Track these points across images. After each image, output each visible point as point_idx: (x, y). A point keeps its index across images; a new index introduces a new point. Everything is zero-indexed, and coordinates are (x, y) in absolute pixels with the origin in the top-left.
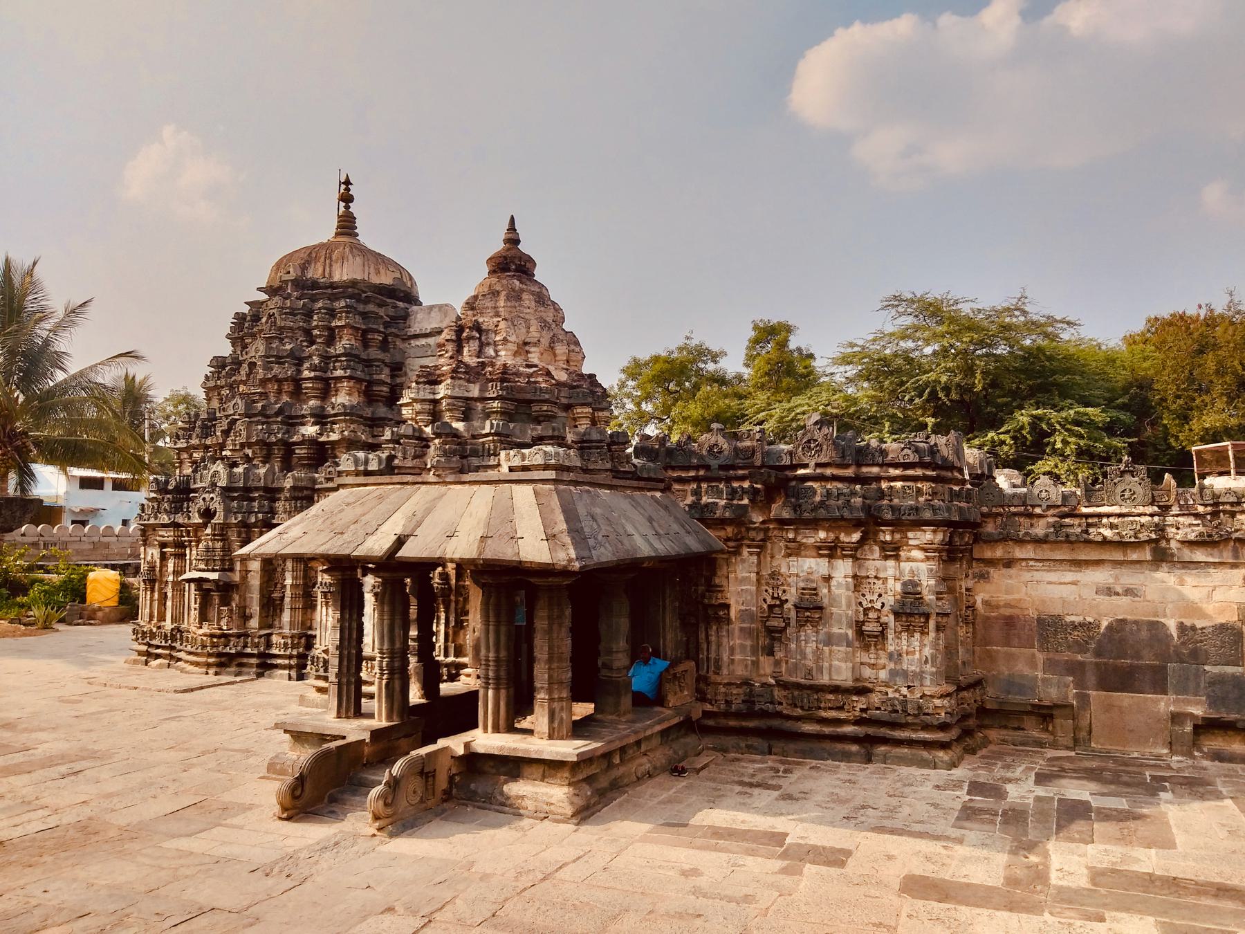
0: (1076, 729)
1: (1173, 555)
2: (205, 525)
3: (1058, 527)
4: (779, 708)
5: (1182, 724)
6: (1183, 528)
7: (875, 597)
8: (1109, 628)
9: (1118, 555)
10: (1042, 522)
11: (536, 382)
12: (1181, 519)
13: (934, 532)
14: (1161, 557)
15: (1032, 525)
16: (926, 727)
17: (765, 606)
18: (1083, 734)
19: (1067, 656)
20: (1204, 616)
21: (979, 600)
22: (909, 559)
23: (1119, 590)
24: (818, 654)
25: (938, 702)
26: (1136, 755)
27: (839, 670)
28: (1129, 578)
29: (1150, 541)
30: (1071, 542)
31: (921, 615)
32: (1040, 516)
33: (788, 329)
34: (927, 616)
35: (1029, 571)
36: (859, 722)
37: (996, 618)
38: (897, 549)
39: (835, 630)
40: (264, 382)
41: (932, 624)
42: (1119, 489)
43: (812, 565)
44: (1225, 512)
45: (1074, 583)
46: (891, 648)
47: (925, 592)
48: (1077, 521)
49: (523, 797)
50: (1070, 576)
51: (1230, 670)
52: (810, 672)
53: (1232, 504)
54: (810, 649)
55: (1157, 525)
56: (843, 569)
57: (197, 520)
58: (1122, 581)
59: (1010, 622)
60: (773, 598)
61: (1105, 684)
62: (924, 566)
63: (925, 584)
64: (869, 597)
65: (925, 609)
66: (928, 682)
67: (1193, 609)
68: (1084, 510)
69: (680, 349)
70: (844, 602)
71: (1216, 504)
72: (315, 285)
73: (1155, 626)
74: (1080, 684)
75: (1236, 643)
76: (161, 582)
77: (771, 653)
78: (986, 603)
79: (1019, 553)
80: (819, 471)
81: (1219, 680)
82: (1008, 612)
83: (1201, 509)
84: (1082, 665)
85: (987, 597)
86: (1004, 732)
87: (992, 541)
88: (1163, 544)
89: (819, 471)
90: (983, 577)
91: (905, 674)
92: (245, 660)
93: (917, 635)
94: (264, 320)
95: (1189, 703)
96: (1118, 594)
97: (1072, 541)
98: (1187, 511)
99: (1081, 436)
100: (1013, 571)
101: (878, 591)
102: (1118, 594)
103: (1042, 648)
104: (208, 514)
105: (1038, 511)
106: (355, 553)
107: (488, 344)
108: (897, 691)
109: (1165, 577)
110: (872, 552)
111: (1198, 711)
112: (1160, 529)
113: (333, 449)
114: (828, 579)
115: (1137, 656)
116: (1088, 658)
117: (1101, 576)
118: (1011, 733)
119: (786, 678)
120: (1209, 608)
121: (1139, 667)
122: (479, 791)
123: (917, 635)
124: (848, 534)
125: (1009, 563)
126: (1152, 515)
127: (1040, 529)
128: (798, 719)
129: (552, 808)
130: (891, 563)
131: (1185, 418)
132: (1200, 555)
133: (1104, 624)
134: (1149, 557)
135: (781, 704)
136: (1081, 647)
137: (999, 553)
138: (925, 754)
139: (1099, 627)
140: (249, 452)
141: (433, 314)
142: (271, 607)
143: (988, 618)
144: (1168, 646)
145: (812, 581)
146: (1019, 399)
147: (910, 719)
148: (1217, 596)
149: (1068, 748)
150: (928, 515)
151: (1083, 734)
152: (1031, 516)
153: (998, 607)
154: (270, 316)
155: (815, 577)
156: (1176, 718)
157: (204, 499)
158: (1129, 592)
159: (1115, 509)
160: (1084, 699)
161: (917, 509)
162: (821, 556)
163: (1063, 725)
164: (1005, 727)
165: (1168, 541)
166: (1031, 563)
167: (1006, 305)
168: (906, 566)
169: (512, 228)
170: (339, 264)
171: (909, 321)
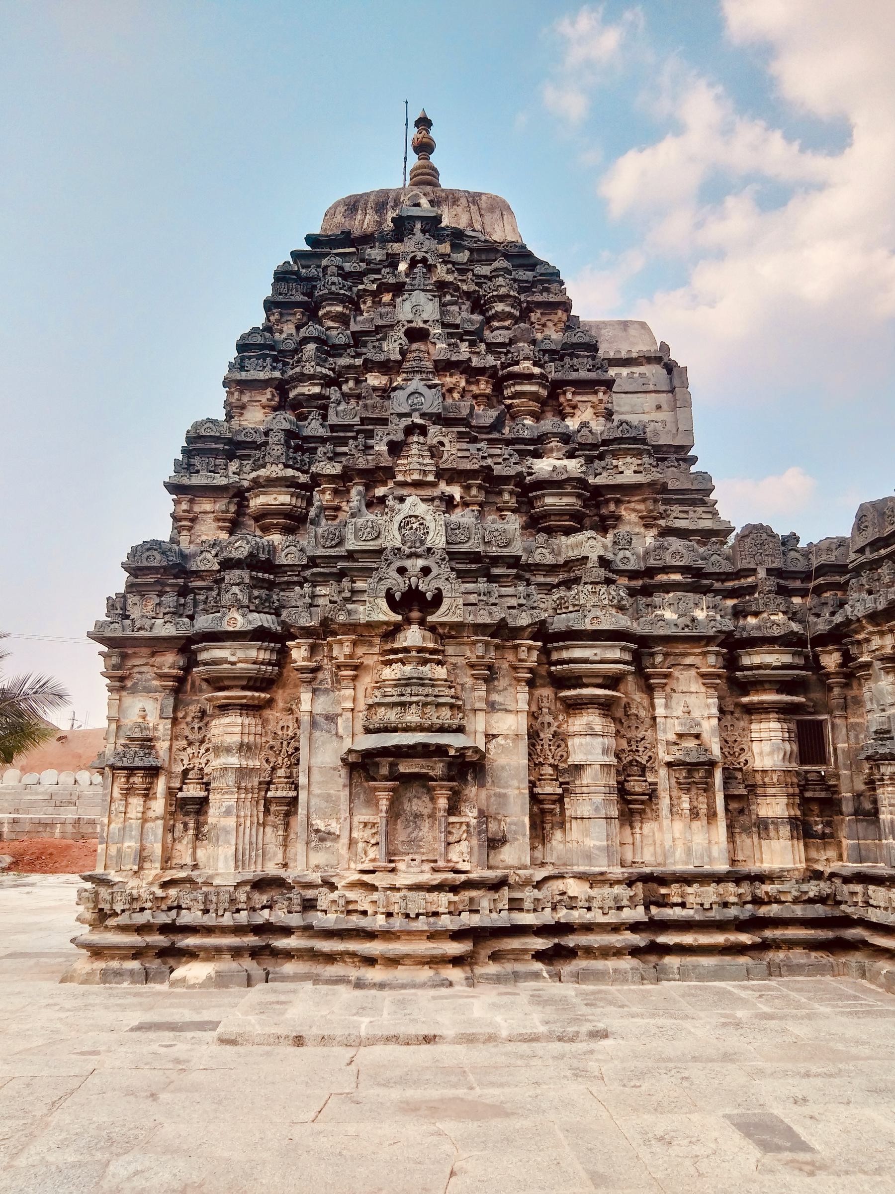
2: (392, 631)
40: (444, 367)
57: (383, 613)
72: (457, 237)
76: (170, 775)
92: (515, 943)
94: (403, 267)
104: (413, 603)
113: (618, 502)
140: (456, 491)
141: (632, 331)
142: (545, 815)
154: (413, 263)
157: (402, 571)
170: (497, 215)
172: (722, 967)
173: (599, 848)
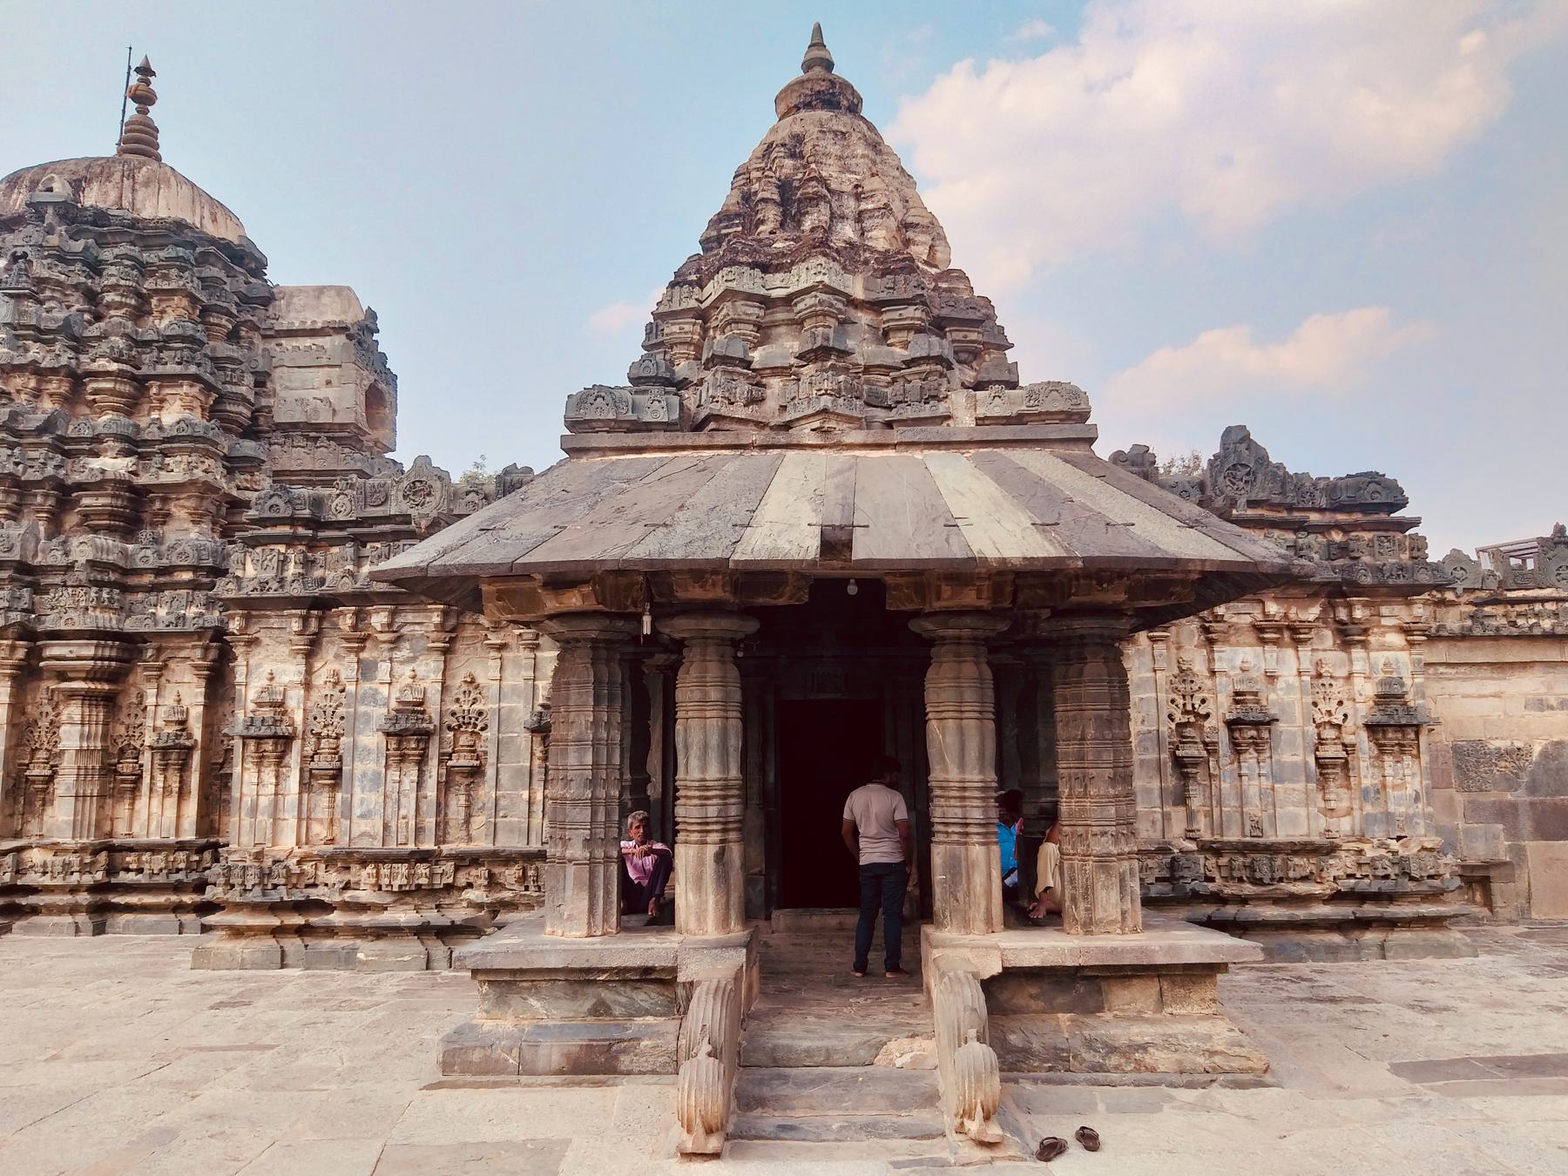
4: (1211, 887)
7: (1333, 706)
8: (1545, 754)
11: (949, 290)
17: (1173, 726)
19: (1493, 796)
22: (1384, 647)
23: (1553, 701)
24: (1268, 796)
27: (1294, 820)
32: (1452, 604)
36: (1337, 897)
38: (1365, 631)
39: (1287, 758)
43: (1241, 658)
46: (1366, 782)
48: (1500, 610)
49: (1143, 1048)
50: (1491, 686)
52: (1257, 826)
54: (1252, 787)
56: (1288, 663)
58: (1557, 690)
60: (1186, 712)
62: (1404, 656)
64: (1323, 706)
70: (1298, 713)
77: (1182, 799)
80: (1250, 512)
89: (1250, 512)
101: (1337, 697)
102: (1551, 708)
105: (1450, 596)
106: (741, 555)
107: (843, 217)
108: (1382, 845)
110: (1321, 638)
114: (1271, 678)
119: (1207, 837)
122: (1036, 1046)
124: (1306, 608)
128: (1244, 901)
129: (1217, 1060)
130: (1357, 653)
133: (1537, 749)
135: (1212, 880)
136: (1512, 785)
139: (1530, 753)
145: (1250, 680)
155: (1254, 674)
162: (1264, 642)
166: (1442, 669)
168: (1380, 657)
169: (818, 43)
172: (158, 923)
173: (66, 822)
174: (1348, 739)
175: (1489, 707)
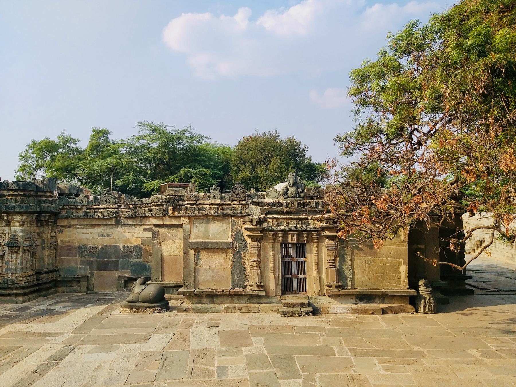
0: (88, 285)
1: (121, 222)
3: (86, 213)
5: (121, 280)
6: (124, 213)
9: (104, 223)
10: (81, 211)
12: (124, 210)
13: (22, 216)
14: (118, 223)
15: (77, 212)
16: (16, 289)
18: (92, 286)
19: (88, 259)
20: (131, 243)
21: (59, 240)
22: (14, 226)
25: (21, 279)
26: (107, 292)
28: (109, 230)
29: (113, 217)
30: (90, 218)
31: (16, 247)
32: (80, 209)
33: (108, 133)
34: (19, 247)
35: (76, 229)
37: (65, 247)
41: (21, 250)
42: (105, 200)
44: (138, 207)
45: (91, 233)
47: (19, 238)
48: (92, 211)
50: (90, 231)
51: (138, 260)
53: (140, 204)
55: (116, 212)
59: (69, 248)
61: (99, 268)
62: (19, 228)
63: (19, 235)
65: (17, 244)
66: (19, 272)
67: (127, 240)
68: (94, 207)
69: (59, 138)
71: (135, 205)
73: (116, 247)
74: (91, 269)
75: (140, 251)
78: (62, 241)
79: (73, 223)
81: (135, 264)
82: (68, 244)
83: (131, 206)
84: (92, 262)
85: (62, 239)
86: (65, 288)
87: (64, 218)
88: (119, 218)
90: (61, 232)
91: (10, 269)
93: (15, 255)
95: (125, 273)
96: (105, 236)
97: (90, 218)
98: (127, 207)
99: (201, 179)
100: (71, 229)
102: (105, 236)
103: (80, 256)
105: (79, 207)
109: (119, 230)
111: (127, 275)
112: (117, 213)
115: (110, 258)
116: (94, 259)
117: (99, 230)
118: (68, 288)
120: (132, 240)
121: (110, 261)
123: (15, 255)
125: (70, 226)
126: (114, 208)
127: (80, 213)
130: (7, 228)
131: (237, 173)
132: (130, 222)
133: (100, 247)
134: (114, 223)
137: (65, 223)
138: (14, 299)
139: (98, 248)
143: (62, 247)
144: (120, 254)
146: (184, 164)
147: (10, 286)
148: (135, 236)
149: (84, 292)
150: (17, 209)
151: (92, 286)
152: (76, 209)
153: (65, 243)
156: (119, 278)
158: (108, 235)
159: (103, 206)
160: (92, 274)
161: (14, 207)
163: (84, 283)
164: (66, 286)
165: (120, 217)
167: (184, 129)
168: (13, 229)
171: (146, 132)
174: (4, 249)
175: (88, 236)
